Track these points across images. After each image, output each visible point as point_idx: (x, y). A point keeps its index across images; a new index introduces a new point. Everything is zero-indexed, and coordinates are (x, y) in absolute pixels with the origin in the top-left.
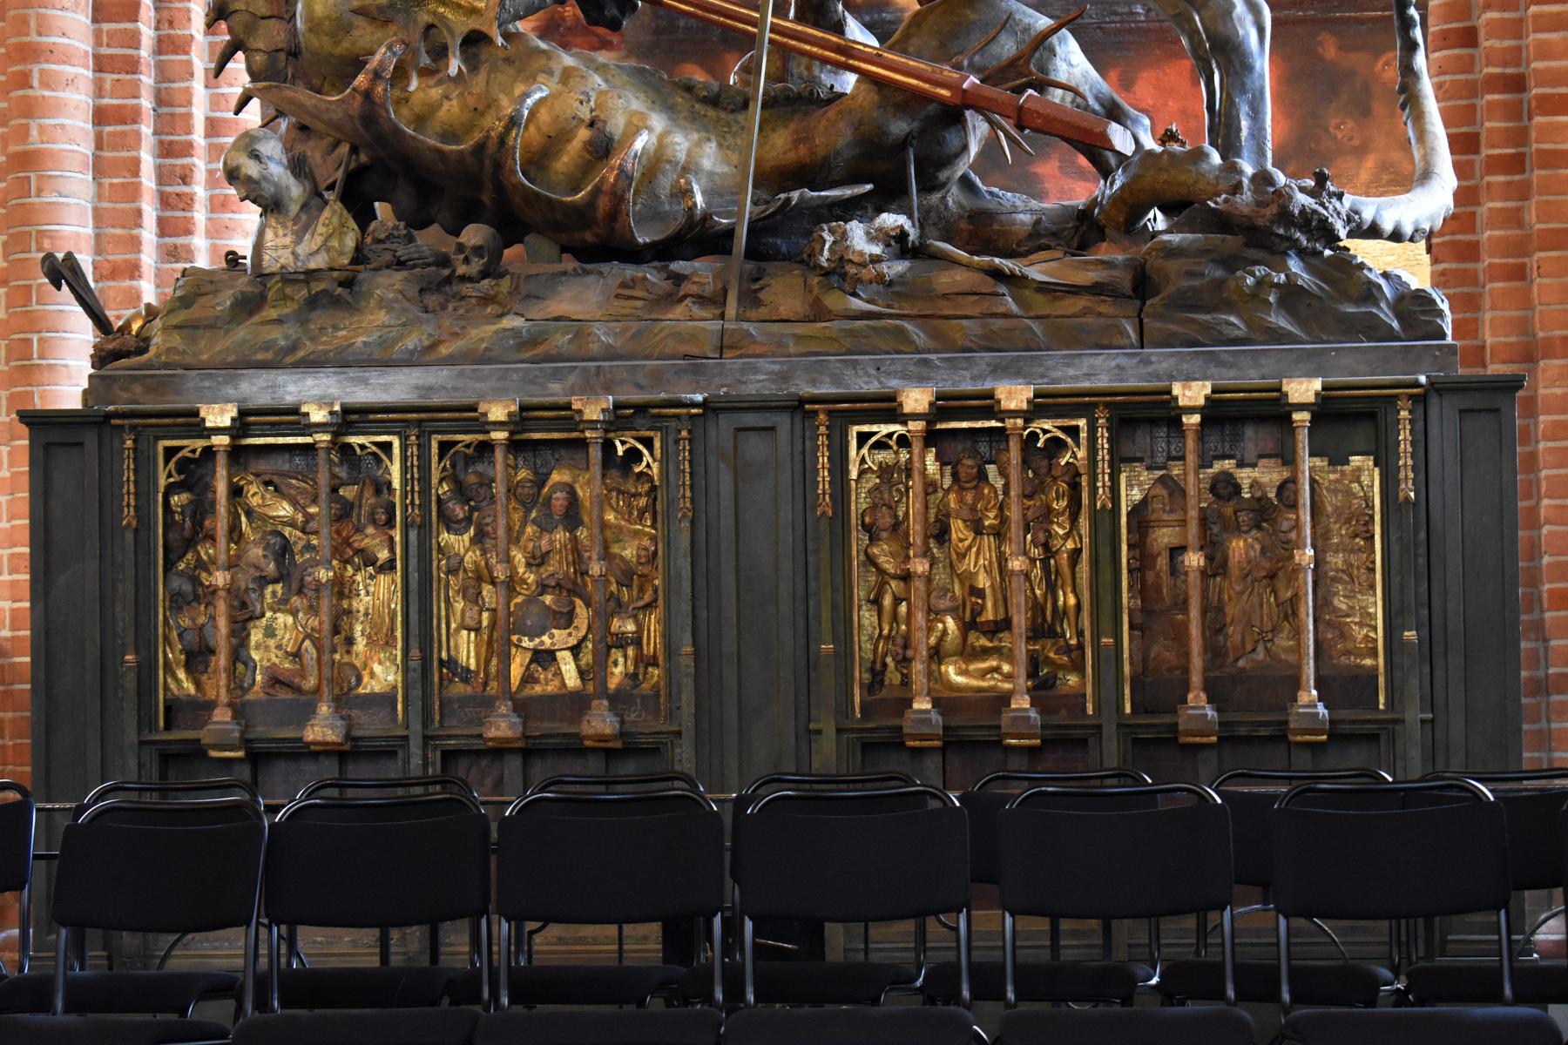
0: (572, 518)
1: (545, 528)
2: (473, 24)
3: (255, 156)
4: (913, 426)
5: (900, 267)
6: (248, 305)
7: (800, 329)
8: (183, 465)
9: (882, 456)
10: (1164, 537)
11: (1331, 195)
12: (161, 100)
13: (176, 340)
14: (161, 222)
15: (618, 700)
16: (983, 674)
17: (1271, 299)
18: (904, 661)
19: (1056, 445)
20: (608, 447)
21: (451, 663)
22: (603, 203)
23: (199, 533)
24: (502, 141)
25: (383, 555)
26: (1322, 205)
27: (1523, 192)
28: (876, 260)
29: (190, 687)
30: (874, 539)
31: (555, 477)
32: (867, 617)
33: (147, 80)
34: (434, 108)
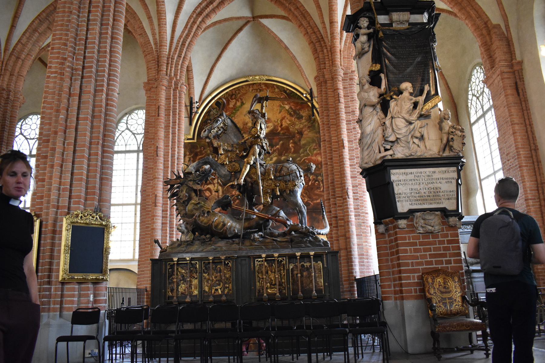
0: (220, 271)
1: (217, 273)
2: (208, 210)
3: (181, 226)
4: (264, 259)
5: (261, 239)
6: (179, 245)
7: (249, 247)
8: (171, 266)
9: (259, 263)
10: (295, 272)
12: (170, 221)
13: (170, 250)
14: (170, 237)
15: (226, 295)
16: (273, 291)
18: (263, 289)
19: (281, 261)
20: (225, 262)
21: (205, 291)
22: (224, 232)
23: (173, 274)
24: (212, 224)
25: (196, 277)
27: (338, 230)
28: (258, 238)
29: (171, 294)
30: (259, 274)
31: (218, 266)
32: (258, 284)
33: (168, 219)
34: (203, 220)
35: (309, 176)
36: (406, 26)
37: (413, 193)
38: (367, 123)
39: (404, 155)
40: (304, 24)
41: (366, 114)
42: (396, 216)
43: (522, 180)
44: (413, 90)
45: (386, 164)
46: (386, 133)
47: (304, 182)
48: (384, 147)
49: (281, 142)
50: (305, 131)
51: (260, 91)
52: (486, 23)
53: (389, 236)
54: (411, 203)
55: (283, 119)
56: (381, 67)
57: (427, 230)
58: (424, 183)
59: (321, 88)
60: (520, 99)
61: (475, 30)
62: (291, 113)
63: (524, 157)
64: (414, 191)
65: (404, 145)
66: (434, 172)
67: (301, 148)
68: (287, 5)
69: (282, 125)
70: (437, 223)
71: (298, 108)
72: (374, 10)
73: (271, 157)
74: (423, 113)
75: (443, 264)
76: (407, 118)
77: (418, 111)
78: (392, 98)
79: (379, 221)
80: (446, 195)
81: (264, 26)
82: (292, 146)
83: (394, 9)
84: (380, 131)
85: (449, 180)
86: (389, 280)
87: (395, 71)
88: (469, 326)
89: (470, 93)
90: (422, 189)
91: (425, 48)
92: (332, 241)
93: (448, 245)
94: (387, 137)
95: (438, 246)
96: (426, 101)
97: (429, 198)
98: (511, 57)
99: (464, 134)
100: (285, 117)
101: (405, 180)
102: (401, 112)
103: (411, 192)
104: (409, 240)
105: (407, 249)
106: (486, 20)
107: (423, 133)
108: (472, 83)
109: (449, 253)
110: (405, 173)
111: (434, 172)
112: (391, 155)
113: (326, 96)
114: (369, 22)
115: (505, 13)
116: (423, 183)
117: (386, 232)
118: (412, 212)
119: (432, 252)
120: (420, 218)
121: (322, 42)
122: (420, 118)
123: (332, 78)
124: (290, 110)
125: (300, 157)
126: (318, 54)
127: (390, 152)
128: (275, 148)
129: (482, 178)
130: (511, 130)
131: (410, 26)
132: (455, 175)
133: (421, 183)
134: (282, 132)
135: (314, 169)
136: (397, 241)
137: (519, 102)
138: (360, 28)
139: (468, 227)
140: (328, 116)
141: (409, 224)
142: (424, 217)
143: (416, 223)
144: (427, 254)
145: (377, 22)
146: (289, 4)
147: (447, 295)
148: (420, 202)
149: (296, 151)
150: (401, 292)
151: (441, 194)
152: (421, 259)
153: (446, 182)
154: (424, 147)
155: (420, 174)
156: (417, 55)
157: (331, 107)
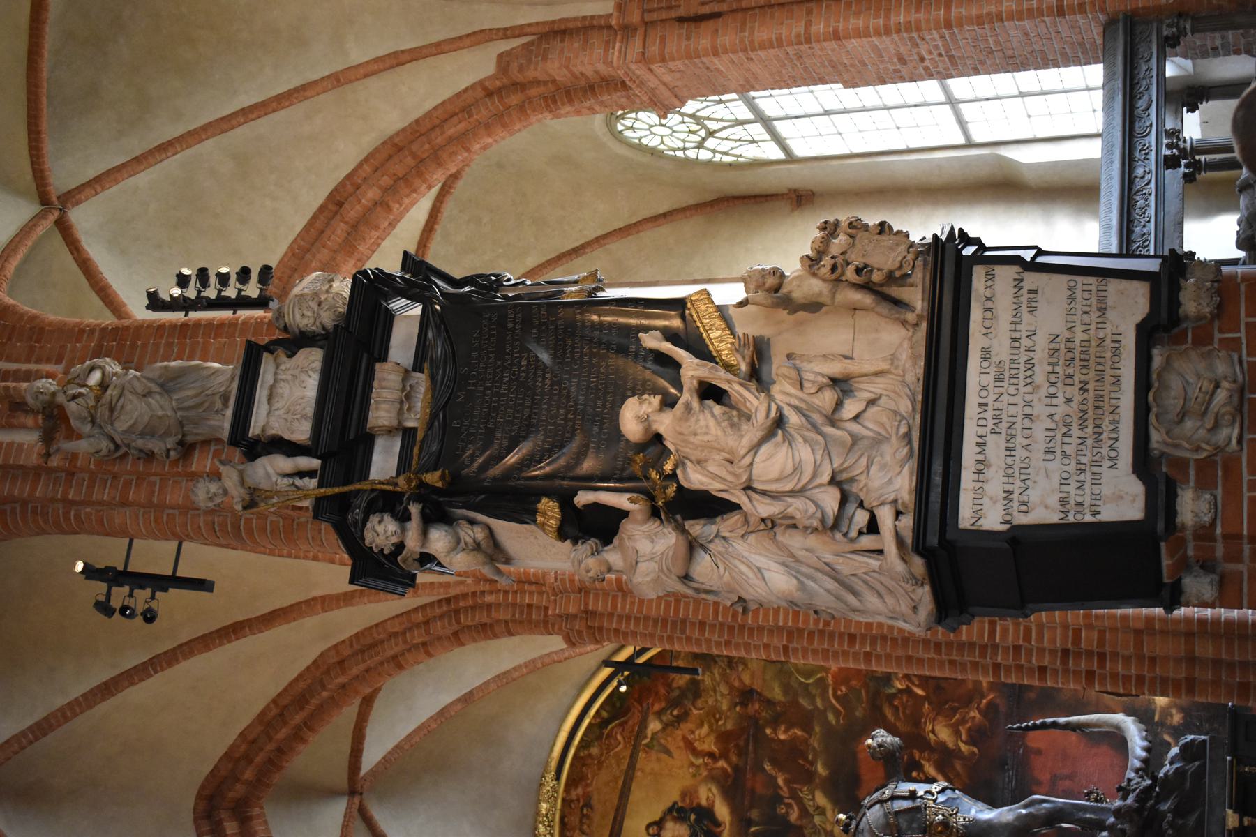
11: (1129, 784)
17: (1180, 822)
26: (1135, 789)
27: (1115, 655)
35: (893, 691)
36: (421, 381)
37: (1066, 448)
38: (754, 581)
39: (902, 466)
40: (396, 650)
41: (721, 577)
43: (991, 22)
44: (654, 392)
45: (933, 540)
46: (807, 523)
47: (935, 788)
48: (860, 533)
49: (768, 767)
50: (741, 680)
51: (588, 805)
52: (489, 94)
53: (1236, 557)
54: (1108, 463)
55: (689, 746)
56: (550, 494)
57: (1228, 409)
58: (1028, 398)
59: (608, 630)
60: (733, 11)
61: (504, 126)
62: (677, 717)
63: (918, 10)
64: (1057, 445)
65: (864, 461)
66: (986, 354)
67: (795, 703)
68: (325, 694)
69: (711, 755)
70: (1201, 366)
71: (662, 691)
72: (346, 489)
73: (811, 810)
74: (744, 367)
76: (759, 434)
77: (737, 387)
78: (673, 476)
80: (1086, 318)
81: (386, 761)
82: (785, 732)
83: (355, 416)
84: (795, 541)
85: (1024, 299)
87: (573, 447)
89: (692, 154)
90: (1052, 410)
91: (510, 325)
92: (1153, 680)
94: (823, 521)
96: (702, 351)
97: (1091, 386)
98: (601, 28)
99: (844, 225)
100: (684, 738)
101: (1008, 476)
102: (731, 452)
103: (1058, 454)
106: (480, 93)
107: (820, 379)
108: (662, 147)
110: (979, 472)
111: (986, 354)
112: (898, 514)
113: (637, 619)
114: (382, 511)
115: (468, 35)
116: (1028, 404)
118: (1144, 463)
120: (1177, 431)
121: (462, 604)
122: (764, 376)
123: (580, 591)
124: (667, 717)
125: (825, 711)
126: (498, 621)
127: (885, 517)
128: (785, 792)
129: (962, 141)
130: (825, 44)
131: (426, 365)
132: (1006, 274)
133: (1028, 410)
134: (734, 759)
135: (889, 739)
137: (740, 15)
138: (400, 546)
139: (1141, 203)
140: (702, 624)
141: (1197, 474)
142: (1172, 416)
143: (1198, 449)
145: (388, 483)
146: (324, 687)
148: (1106, 427)
149: (806, 721)
151: (1079, 336)
153: (1032, 310)
154: (878, 380)
155: (990, 408)
156: (528, 359)
157: (677, 611)
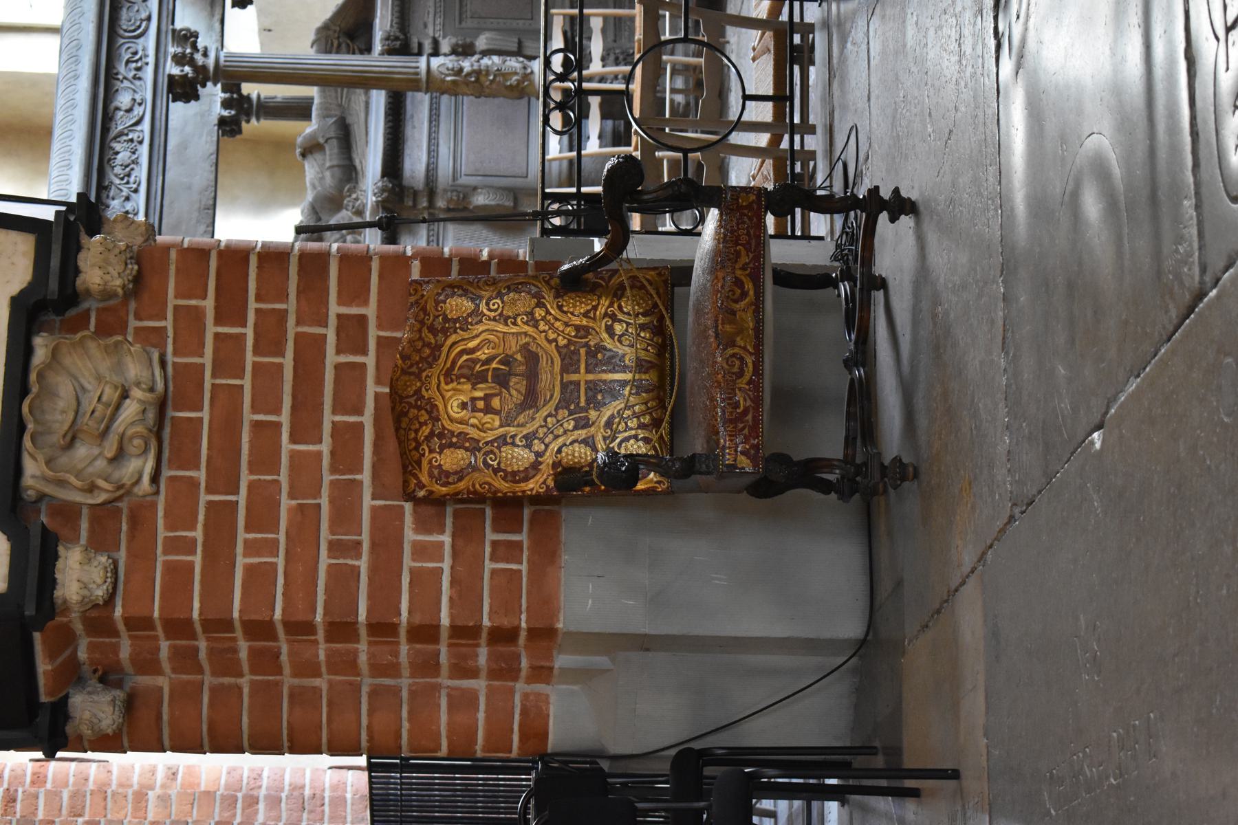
42: (30, 611)
53: (149, 665)
57: (139, 429)
70: (104, 365)
75: (363, 366)
79: (43, 720)
86: (423, 698)
88: (738, 283)
93: (251, 317)
95: (247, 382)
104: (190, 546)
105: (250, 570)
109: (299, 322)
117: (119, 685)
119: (285, 418)
120: (64, 460)
136: (189, 622)
139: (123, 157)
141: (92, 531)
142: (56, 438)
143: (92, 488)
144: (293, 455)
147: (545, 377)
150: (503, 636)
152: (318, 494)
